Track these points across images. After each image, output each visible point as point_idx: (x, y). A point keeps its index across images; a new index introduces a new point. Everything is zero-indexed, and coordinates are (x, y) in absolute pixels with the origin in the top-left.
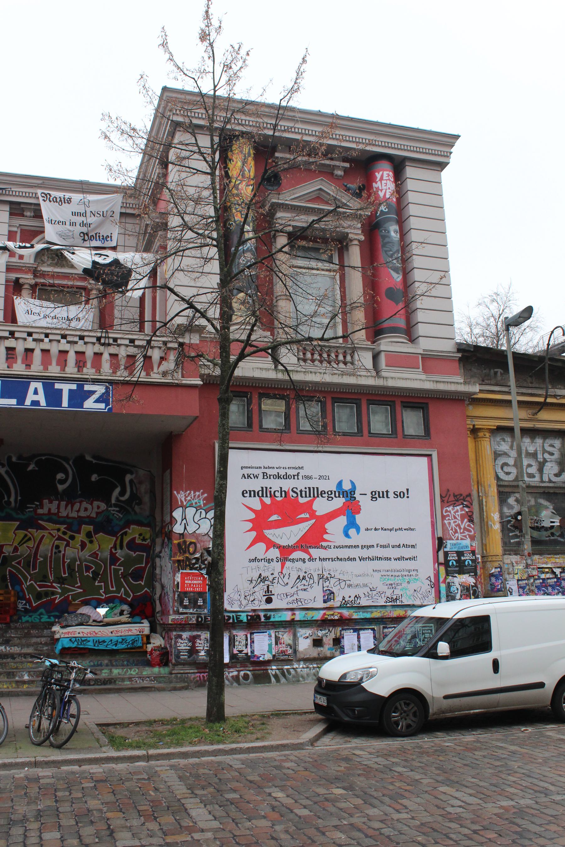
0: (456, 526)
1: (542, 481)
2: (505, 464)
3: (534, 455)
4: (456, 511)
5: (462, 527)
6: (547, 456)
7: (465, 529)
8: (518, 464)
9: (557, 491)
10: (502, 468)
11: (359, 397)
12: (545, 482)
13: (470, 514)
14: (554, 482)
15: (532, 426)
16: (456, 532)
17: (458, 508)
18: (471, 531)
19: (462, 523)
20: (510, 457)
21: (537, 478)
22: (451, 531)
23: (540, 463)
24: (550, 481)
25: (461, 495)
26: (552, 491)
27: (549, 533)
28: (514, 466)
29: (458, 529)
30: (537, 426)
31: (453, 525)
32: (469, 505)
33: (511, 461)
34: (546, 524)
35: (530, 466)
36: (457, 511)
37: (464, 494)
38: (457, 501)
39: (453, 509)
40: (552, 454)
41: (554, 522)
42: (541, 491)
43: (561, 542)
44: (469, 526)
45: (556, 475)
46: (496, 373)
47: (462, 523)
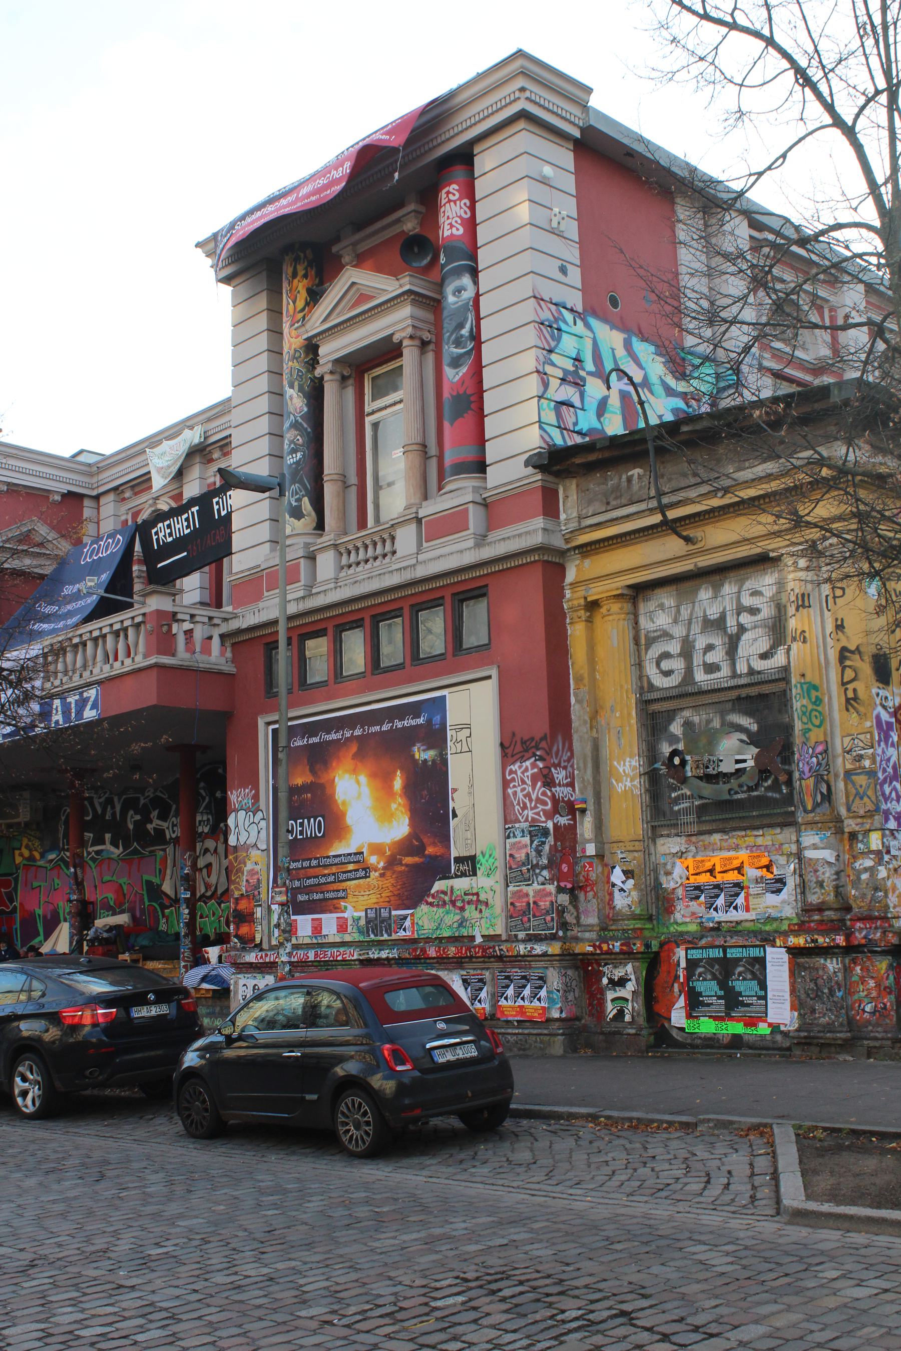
0: (525, 796)
1: (734, 675)
2: (666, 655)
3: (719, 624)
4: (525, 769)
5: (534, 797)
6: (745, 619)
7: (538, 799)
8: (687, 652)
9: (766, 689)
10: (658, 665)
11: (360, 616)
12: (740, 676)
13: (545, 772)
14: (759, 673)
15: (691, 567)
16: (525, 807)
17: (528, 763)
18: (546, 804)
19: (534, 789)
20: (672, 637)
21: (725, 671)
22: (517, 807)
23: (731, 637)
24: (751, 672)
25: (532, 739)
26: (753, 691)
27: (734, 783)
28: (680, 655)
29: (527, 801)
30: (700, 565)
31: (520, 795)
32: (545, 756)
33: (674, 647)
34: (728, 767)
35: (710, 648)
36: (526, 770)
37: (537, 738)
38: (526, 751)
39: (520, 767)
40: (754, 611)
41: (744, 761)
42: (734, 694)
43: (775, 799)
44: (544, 794)
45: (764, 656)
46: (629, 480)
47: (534, 789)
